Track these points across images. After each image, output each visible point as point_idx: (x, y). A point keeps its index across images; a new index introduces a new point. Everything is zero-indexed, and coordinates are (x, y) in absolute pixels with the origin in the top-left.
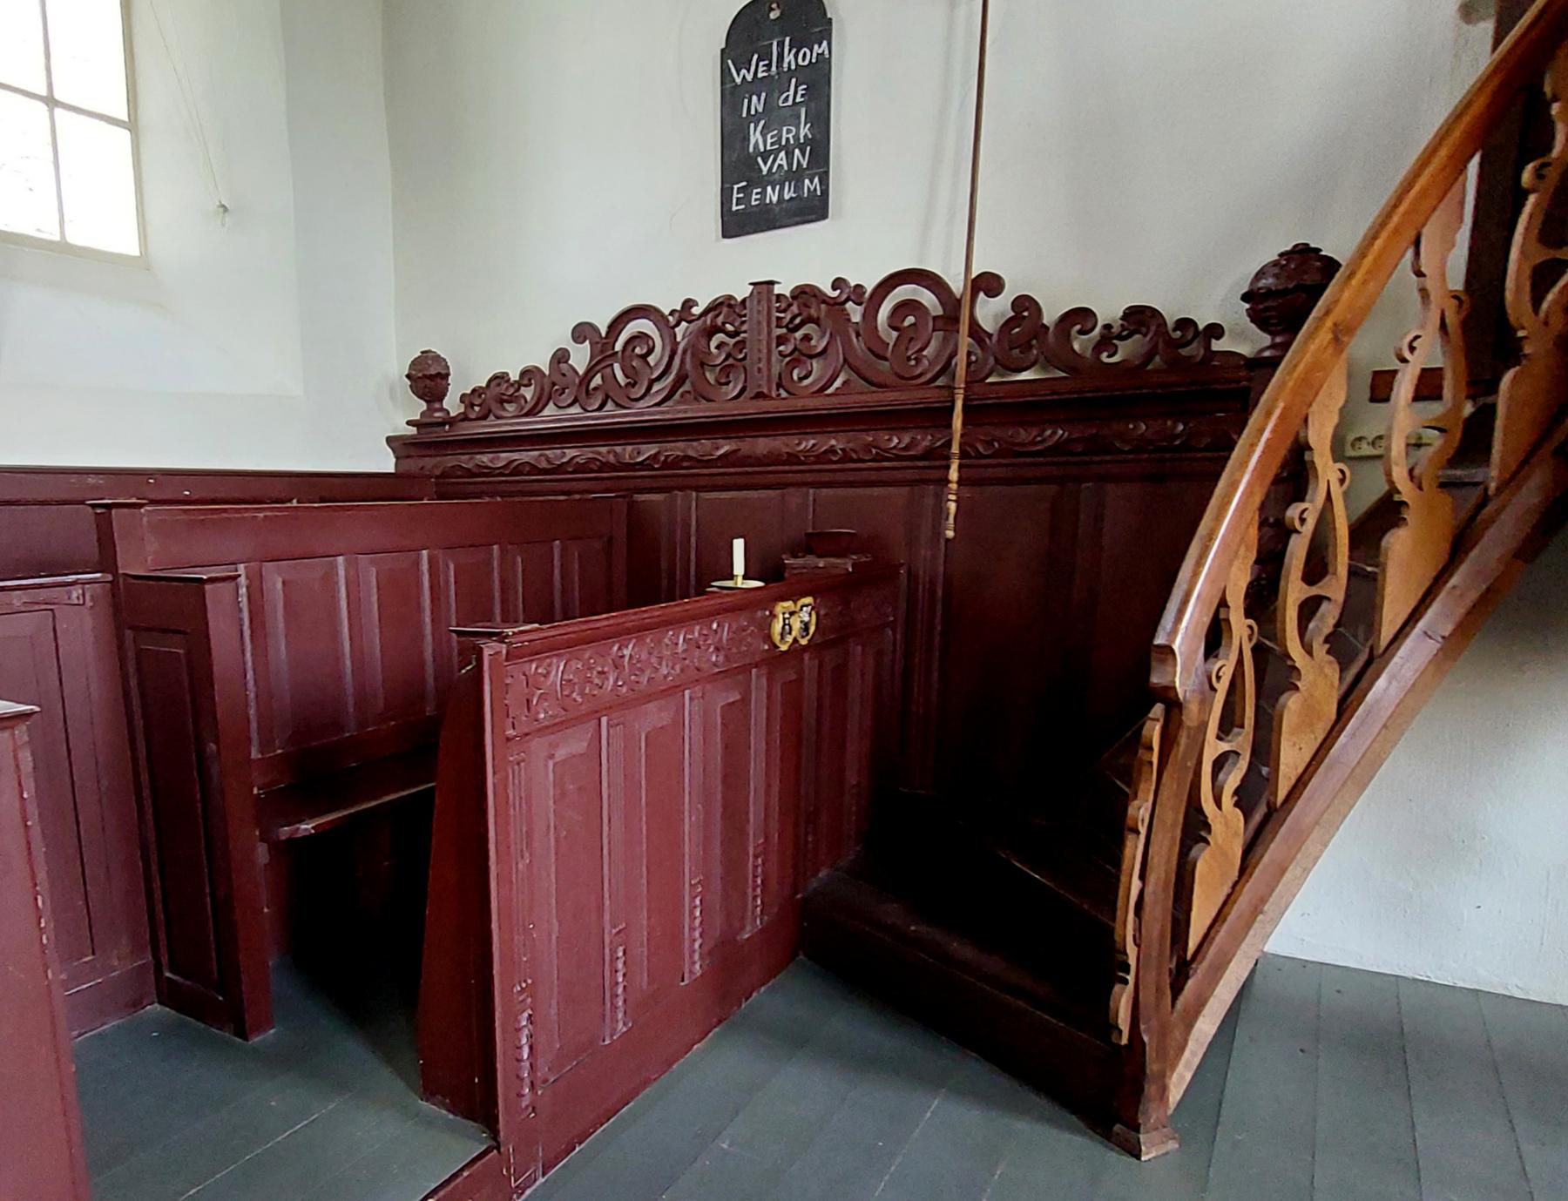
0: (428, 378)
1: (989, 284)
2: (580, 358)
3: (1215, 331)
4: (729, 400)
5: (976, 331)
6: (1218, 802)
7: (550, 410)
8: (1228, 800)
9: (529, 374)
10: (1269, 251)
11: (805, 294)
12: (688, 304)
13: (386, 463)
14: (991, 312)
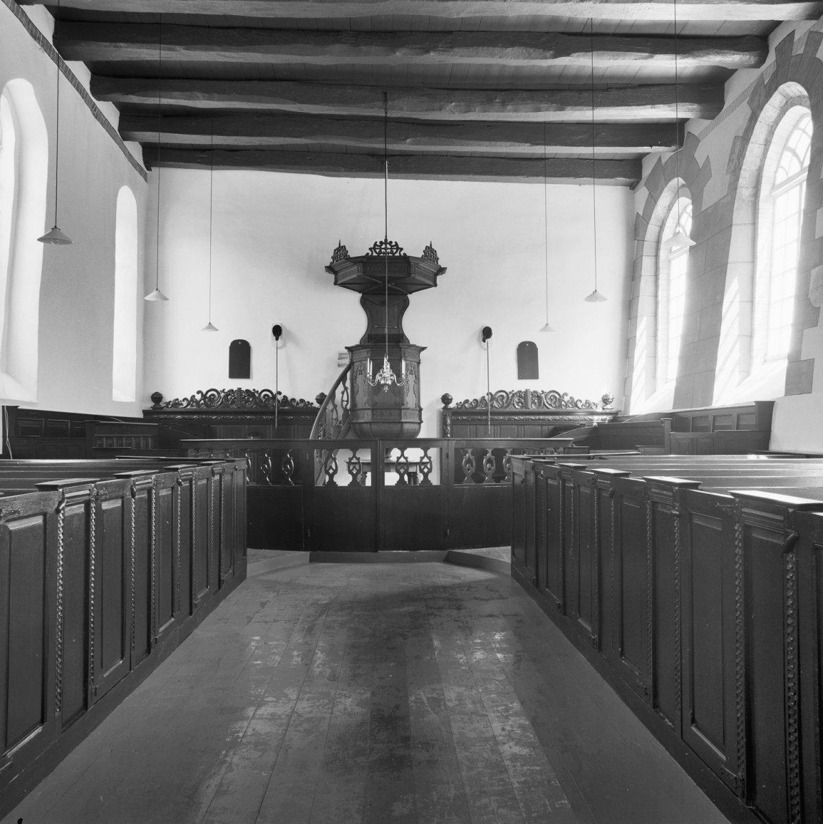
0: (157, 398)
2: (198, 397)
3: (312, 403)
5: (278, 401)
9: (185, 399)
10: (318, 393)
11: (248, 391)
12: (224, 390)
13: (141, 416)
14: (280, 397)
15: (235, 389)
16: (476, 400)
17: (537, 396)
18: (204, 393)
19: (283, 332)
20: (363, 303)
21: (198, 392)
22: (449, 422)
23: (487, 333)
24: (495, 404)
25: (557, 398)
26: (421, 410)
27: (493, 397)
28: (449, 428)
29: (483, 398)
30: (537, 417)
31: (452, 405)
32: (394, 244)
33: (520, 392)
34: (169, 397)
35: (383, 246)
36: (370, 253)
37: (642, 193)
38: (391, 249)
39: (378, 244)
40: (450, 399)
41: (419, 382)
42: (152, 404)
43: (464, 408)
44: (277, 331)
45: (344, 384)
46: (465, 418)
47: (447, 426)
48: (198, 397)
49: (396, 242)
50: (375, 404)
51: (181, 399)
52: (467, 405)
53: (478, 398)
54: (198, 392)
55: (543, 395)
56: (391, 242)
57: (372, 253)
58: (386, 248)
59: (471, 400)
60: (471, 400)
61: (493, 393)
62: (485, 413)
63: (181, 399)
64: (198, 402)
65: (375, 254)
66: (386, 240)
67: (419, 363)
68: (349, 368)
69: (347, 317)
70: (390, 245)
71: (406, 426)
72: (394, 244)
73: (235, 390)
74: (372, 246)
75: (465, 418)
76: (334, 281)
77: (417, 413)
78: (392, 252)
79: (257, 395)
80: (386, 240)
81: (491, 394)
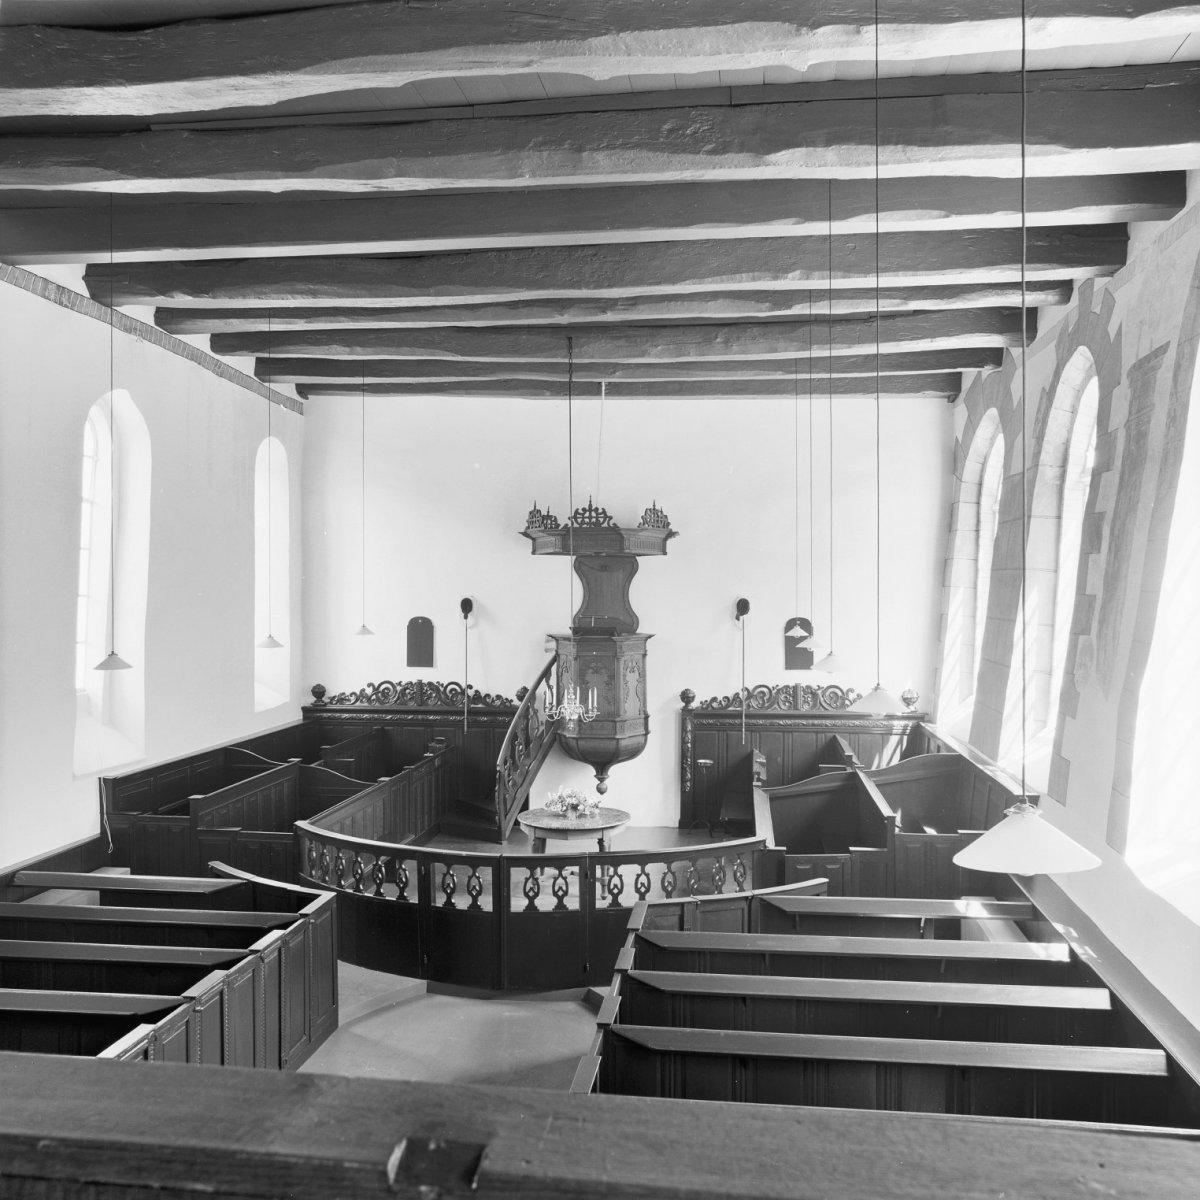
0: (319, 692)
1: (470, 687)
2: (369, 691)
3: (512, 701)
4: (412, 705)
5: (468, 696)
7: (358, 703)
11: (430, 684)
14: (471, 693)
15: (414, 681)
16: (726, 697)
17: (812, 693)
18: (376, 685)
19: (475, 606)
20: (578, 567)
21: (369, 685)
22: (689, 728)
23: (743, 607)
24: (754, 703)
25: (839, 696)
26: (647, 718)
27: (750, 695)
28: (690, 736)
29: (737, 694)
30: (810, 722)
31: (695, 705)
32: (600, 511)
33: (787, 687)
34: (333, 690)
35: (587, 514)
37: (961, 410)
38: (597, 518)
41: (645, 680)
42: (313, 699)
43: (710, 709)
44: (467, 606)
45: (547, 682)
46: (711, 721)
47: (687, 732)
48: (369, 691)
51: (348, 693)
52: (715, 705)
53: (730, 695)
54: (369, 685)
55: (819, 692)
56: (597, 509)
58: (590, 517)
59: (720, 698)
60: (720, 698)
61: (751, 688)
62: (739, 715)
63: (348, 693)
64: (369, 699)
65: (576, 525)
66: (590, 505)
67: (645, 655)
68: (554, 660)
69: (556, 591)
71: (623, 743)
72: (600, 511)
75: (711, 721)
76: (531, 550)
77: (642, 721)
79: (442, 689)
80: (590, 505)
81: (747, 689)
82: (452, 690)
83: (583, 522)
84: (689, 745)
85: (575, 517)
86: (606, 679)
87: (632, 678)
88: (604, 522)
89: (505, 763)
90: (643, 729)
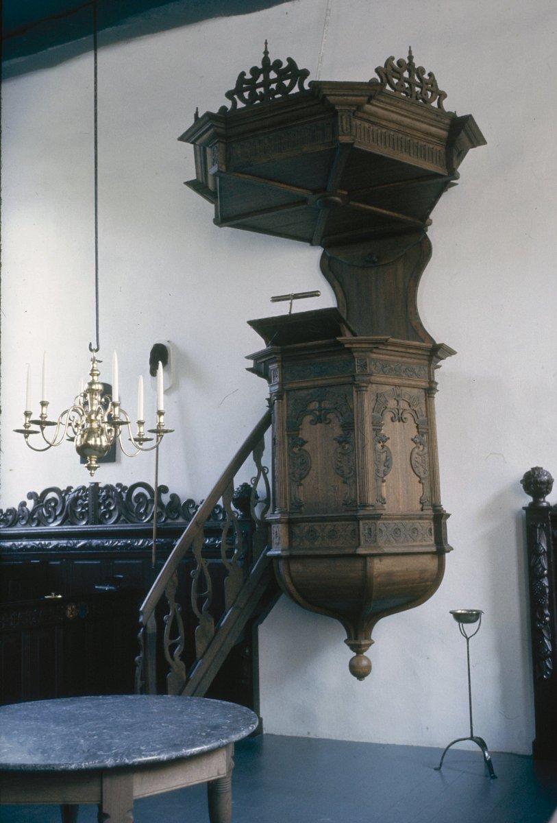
1: (163, 489)
2: (30, 505)
6: (173, 659)
8: (177, 659)
11: (109, 488)
14: (166, 499)
26: (439, 518)
28: (544, 563)
32: (285, 64)
35: (261, 79)
36: (229, 104)
39: (248, 76)
40: (542, 483)
44: (159, 354)
49: (289, 60)
50: (297, 506)
56: (278, 63)
57: (235, 104)
65: (240, 105)
66: (266, 60)
70: (276, 72)
73: (87, 486)
74: (233, 87)
77: (428, 524)
78: (281, 89)
82: (140, 495)
83: (253, 96)
84: (546, 582)
85: (238, 91)
86: (338, 431)
87: (399, 436)
88: (291, 86)
89: (161, 607)
90: (431, 540)
